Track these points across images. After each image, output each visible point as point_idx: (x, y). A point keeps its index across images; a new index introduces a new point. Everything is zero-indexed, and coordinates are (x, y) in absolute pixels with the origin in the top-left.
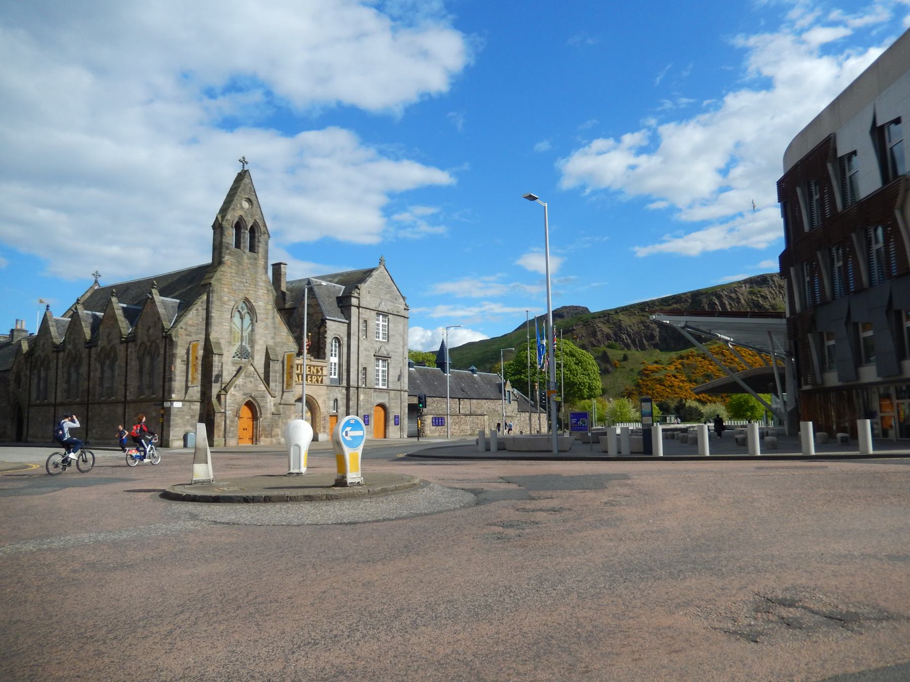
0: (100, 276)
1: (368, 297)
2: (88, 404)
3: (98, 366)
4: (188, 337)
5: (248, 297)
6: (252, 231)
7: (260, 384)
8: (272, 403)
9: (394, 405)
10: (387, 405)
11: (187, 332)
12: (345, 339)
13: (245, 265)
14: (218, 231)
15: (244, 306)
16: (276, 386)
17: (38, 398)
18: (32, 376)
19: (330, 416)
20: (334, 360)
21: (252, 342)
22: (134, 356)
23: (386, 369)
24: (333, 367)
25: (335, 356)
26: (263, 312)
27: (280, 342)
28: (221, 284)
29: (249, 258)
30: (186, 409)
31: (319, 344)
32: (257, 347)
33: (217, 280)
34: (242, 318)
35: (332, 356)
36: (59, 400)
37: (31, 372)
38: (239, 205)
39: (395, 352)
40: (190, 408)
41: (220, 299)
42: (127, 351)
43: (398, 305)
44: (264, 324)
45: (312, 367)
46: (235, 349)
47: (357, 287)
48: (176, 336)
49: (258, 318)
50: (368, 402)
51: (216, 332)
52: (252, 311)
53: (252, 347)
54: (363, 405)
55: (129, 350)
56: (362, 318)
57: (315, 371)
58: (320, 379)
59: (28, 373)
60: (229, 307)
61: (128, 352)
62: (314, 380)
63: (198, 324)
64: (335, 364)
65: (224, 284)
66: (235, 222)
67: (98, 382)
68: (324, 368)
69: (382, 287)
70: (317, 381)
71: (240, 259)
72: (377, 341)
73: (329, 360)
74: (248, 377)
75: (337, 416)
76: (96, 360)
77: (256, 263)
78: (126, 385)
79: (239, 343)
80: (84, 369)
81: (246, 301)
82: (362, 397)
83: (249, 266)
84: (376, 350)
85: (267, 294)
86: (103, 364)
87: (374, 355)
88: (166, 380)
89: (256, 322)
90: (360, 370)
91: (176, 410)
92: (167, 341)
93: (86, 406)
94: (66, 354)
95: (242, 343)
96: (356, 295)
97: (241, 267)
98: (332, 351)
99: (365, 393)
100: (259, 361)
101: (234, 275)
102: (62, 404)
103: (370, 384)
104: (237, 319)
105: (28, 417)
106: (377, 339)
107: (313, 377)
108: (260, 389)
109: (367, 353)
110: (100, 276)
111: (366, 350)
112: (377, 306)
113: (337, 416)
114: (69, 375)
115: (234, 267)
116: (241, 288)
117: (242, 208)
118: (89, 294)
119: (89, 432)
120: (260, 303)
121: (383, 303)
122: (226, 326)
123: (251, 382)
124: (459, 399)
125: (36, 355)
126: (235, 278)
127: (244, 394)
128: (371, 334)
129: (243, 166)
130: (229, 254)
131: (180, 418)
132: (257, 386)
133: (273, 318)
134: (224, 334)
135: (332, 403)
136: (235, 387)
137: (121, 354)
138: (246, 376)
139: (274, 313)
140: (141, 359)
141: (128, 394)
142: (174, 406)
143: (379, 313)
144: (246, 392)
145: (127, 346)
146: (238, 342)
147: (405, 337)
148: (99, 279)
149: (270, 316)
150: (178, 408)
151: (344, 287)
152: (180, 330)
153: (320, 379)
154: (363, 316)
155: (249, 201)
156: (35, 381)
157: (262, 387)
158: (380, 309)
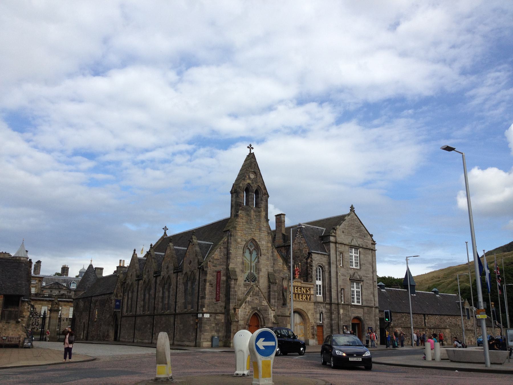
0: (167, 229)
2: (154, 316)
3: (161, 289)
4: (214, 268)
5: (255, 238)
6: (257, 192)
7: (264, 300)
8: (272, 315)
9: (368, 318)
10: (362, 318)
11: (214, 264)
12: (327, 267)
13: (252, 216)
14: (234, 195)
15: (252, 245)
16: (275, 302)
17: (127, 312)
18: (124, 297)
19: (318, 326)
20: (319, 283)
21: (258, 270)
22: (181, 281)
23: (360, 290)
24: (318, 288)
25: (320, 280)
26: (265, 248)
27: (277, 270)
28: (236, 230)
29: (255, 211)
30: (212, 319)
31: (307, 271)
32: (261, 274)
33: (233, 227)
34: (251, 253)
35: (317, 280)
36: (138, 313)
37: (123, 294)
38: (247, 176)
40: (215, 318)
41: (236, 241)
42: (177, 279)
44: (266, 257)
45: (302, 289)
46: (246, 275)
47: (334, 229)
48: (207, 267)
49: (262, 253)
50: (346, 315)
51: (233, 263)
52: (257, 248)
53: (258, 273)
55: (178, 278)
56: (339, 251)
57: (305, 292)
58: (308, 297)
59: (122, 295)
60: (242, 246)
61: (178, 279)
62: (304, 298)
63: (221, 258)
64: (320, 286)
65: (238, 230)
66: (245, 188)
67: (160, 300)
68: (311, 289)
70: (307, 298)
71: (249, 213)
72: (351, 268)
73: (315, 283)
74: (255, 295)
75: (322, 326)
76: (159, 285)
77: (260, 215)
78: (176, 302)
79: (249, 271)
80: (152, 292)
81: (253, 240)
82: (341, 311)
83: (255, 217)
84: (350, 275)
85: (268, 236)
86: (163, 288)
87: (350, 279)
88: (200, 298)
89: (261, 255)
90: (339, 290)
91: (206, 319)
92: (201, 271)
93: (153, 317)
94: (143, 281)
95: (251, 271)
96: (333, 234)
97: (249, 218)
98: (317, 276)
99: (343, 309)
100: (263, 282)
101: (245, 224)
102: (140, 316)
103: (347, 302)
104: (247, 254)
105: (121, 325)
106: (351, 267)
107: (303, 295)
108: (263, 304)
109: (344, 277)
110: (167, 229)
111: (343, 275)
112: (350, 242)
114: (145, 295)
115: (244, 218)
116: (249, 232)
117: (249, 178)
118: (160, 241)
119: (154, 335)
120: (264, 243)
121: (354, 240)
122: (240, 260)
123: (257, 299)
124: (424, 315)
125: (127, 282)
126: (246, 226)
127: (253, 308)
128: (346, 263)
129: (250, 150)
130: (241, 209)
131: (208, 326)
132: (261, 302)
133: (272, 252)
134: (238, 265)
135: (318, 316)
136: (245, 303)
137: (174, 281)
138: (253, 295)
139: (273, 249)
140: (186, 284)
141: (177, 308)
142: (204, 317)
143: (352, 247)
144: (253, 306)
145: (177, 275)
146: (248, 270)
147: (374, 265)
148: (167, 231)
149: (270, 251)
150: (206, 318)
151: (325, 229)
152: (209, 262)
153: (308, 297)
154: (339, 250)
155: (255, 173)
156: (126, 300)
157: (265, 303)
158: (352, 244)
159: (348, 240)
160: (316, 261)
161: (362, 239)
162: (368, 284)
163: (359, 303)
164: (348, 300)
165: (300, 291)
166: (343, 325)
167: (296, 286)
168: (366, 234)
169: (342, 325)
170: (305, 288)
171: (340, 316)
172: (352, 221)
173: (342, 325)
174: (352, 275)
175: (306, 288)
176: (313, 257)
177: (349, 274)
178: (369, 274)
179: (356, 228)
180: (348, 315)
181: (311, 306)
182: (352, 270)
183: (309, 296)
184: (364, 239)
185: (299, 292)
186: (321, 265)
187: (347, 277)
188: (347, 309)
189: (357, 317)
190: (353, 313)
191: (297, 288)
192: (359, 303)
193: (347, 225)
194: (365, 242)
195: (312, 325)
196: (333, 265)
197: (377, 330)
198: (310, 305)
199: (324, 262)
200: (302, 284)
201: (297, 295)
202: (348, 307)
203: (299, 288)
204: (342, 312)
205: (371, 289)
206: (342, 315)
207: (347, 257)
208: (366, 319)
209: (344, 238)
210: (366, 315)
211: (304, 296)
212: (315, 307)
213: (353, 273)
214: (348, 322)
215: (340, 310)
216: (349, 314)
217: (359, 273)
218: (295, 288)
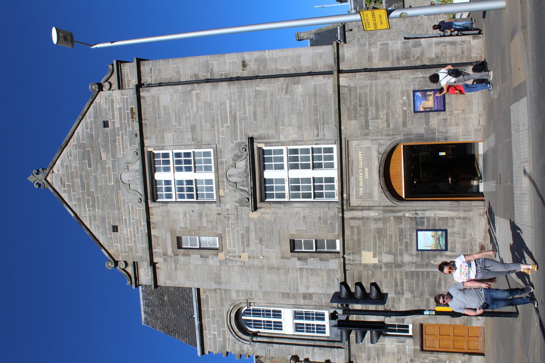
1: (124, 231)
9: (382, 114)
23: (284, 148)
39: (234, 119)
43: (116, 113)
50: (380, 233)
54: (390, 253)
69: (92, 178)
103: (332, 225)
109: (252, 235)
111: (246, 243)
113: (422, 325)
159: (132, 207)
160: (224, 339)
161: (114, 141)
162: (260, 111)
163: (330, 150)
164: (325, 222)
166: (414, 252)
168: (96, 117)
169: (415, 259)
171: (387, 264)
172: (73, 183)
173: (415, 259)
174: (238, 195)
176: (215, 348)
177: (237, 209)
178: (223, 104)
179: (90, 166)
180: (380, 225)
182: (221, 191)
184: (114, 129)
186: (233, 315)
187: (249, 219)
188: (358, 228)
189: (382, 170)
190: (371, 195)
192: (330, 150)
193: (89, 210)
194: (121, 125)
196: (223, 280)
197: (423, 53)
199: (222, 305)
202: (353, 223)
204: (372, 253)
205: (272, 95)
206: (380, 254)
207: (185, 214)
208: (385, 125)
209: (130, 228)
210: (371, 123)
212: (364, 355)
213: (231, 188)
214: (402, 226)
215: (366, 266)
216: (376, 220)
217: (227, 157)
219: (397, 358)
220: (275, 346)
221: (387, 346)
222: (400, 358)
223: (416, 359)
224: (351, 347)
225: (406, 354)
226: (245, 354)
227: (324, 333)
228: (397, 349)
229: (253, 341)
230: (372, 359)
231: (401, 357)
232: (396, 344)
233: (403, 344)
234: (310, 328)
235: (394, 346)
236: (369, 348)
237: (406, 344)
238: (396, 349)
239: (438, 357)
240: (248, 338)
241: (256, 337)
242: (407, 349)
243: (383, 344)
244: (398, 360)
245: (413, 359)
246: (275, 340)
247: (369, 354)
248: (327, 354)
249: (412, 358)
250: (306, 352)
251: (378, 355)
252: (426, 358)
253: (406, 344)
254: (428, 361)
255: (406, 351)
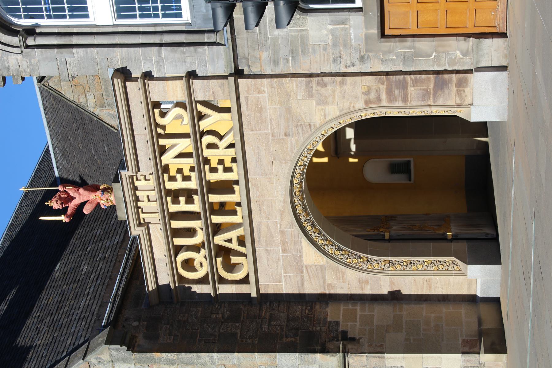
165: (190, 201)
167: (163, 206)
170: (162, 142)
175: (160, 136)
181: (265, 98)
183: (200, 108)
185: (193, 184)
191: (176, 201)
195: (384, 96)
198: (259, 108)
200: (143, 171)
201: (216, 219)
203: (170, 185)
211: (211, 146)
218: (173, 208)
219: (332, 57)
220: (78, 53)
221: (311, 33)
222: (338, 55)
223: (370, 54)
224: (238, 42)
225: (351, 45)
226: (13, 75)
227: (180, 16)
228: (333, 39)
229: (28, 47)
230: (281, 62)
231: (340, 53)
232: (330, 27)
233: (343, 26)
234: (148, 9)
235: (324, 32)
236: (275, 41)
237: (350, 27)
238: (331, 37)
239: (414, 48)
240: (15, 40)
241: (33, 38)
242: (352, 37)
243: (303, 30)
244: (335, 60)
245: (365, 55)
246: (75, 40)
247: (275, 52)
248: (189, 60)
249: (362, 54)
250: (145, 59)
251: (293, 53)
252: (390, 52)
253: (350, 27)
254: (395, 57)
255: (351, 39)
